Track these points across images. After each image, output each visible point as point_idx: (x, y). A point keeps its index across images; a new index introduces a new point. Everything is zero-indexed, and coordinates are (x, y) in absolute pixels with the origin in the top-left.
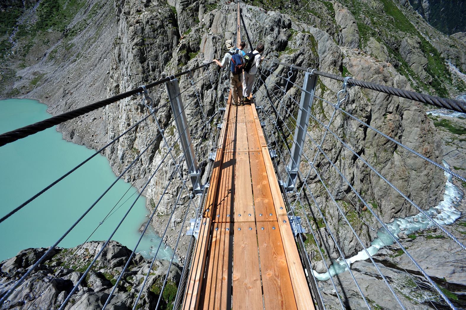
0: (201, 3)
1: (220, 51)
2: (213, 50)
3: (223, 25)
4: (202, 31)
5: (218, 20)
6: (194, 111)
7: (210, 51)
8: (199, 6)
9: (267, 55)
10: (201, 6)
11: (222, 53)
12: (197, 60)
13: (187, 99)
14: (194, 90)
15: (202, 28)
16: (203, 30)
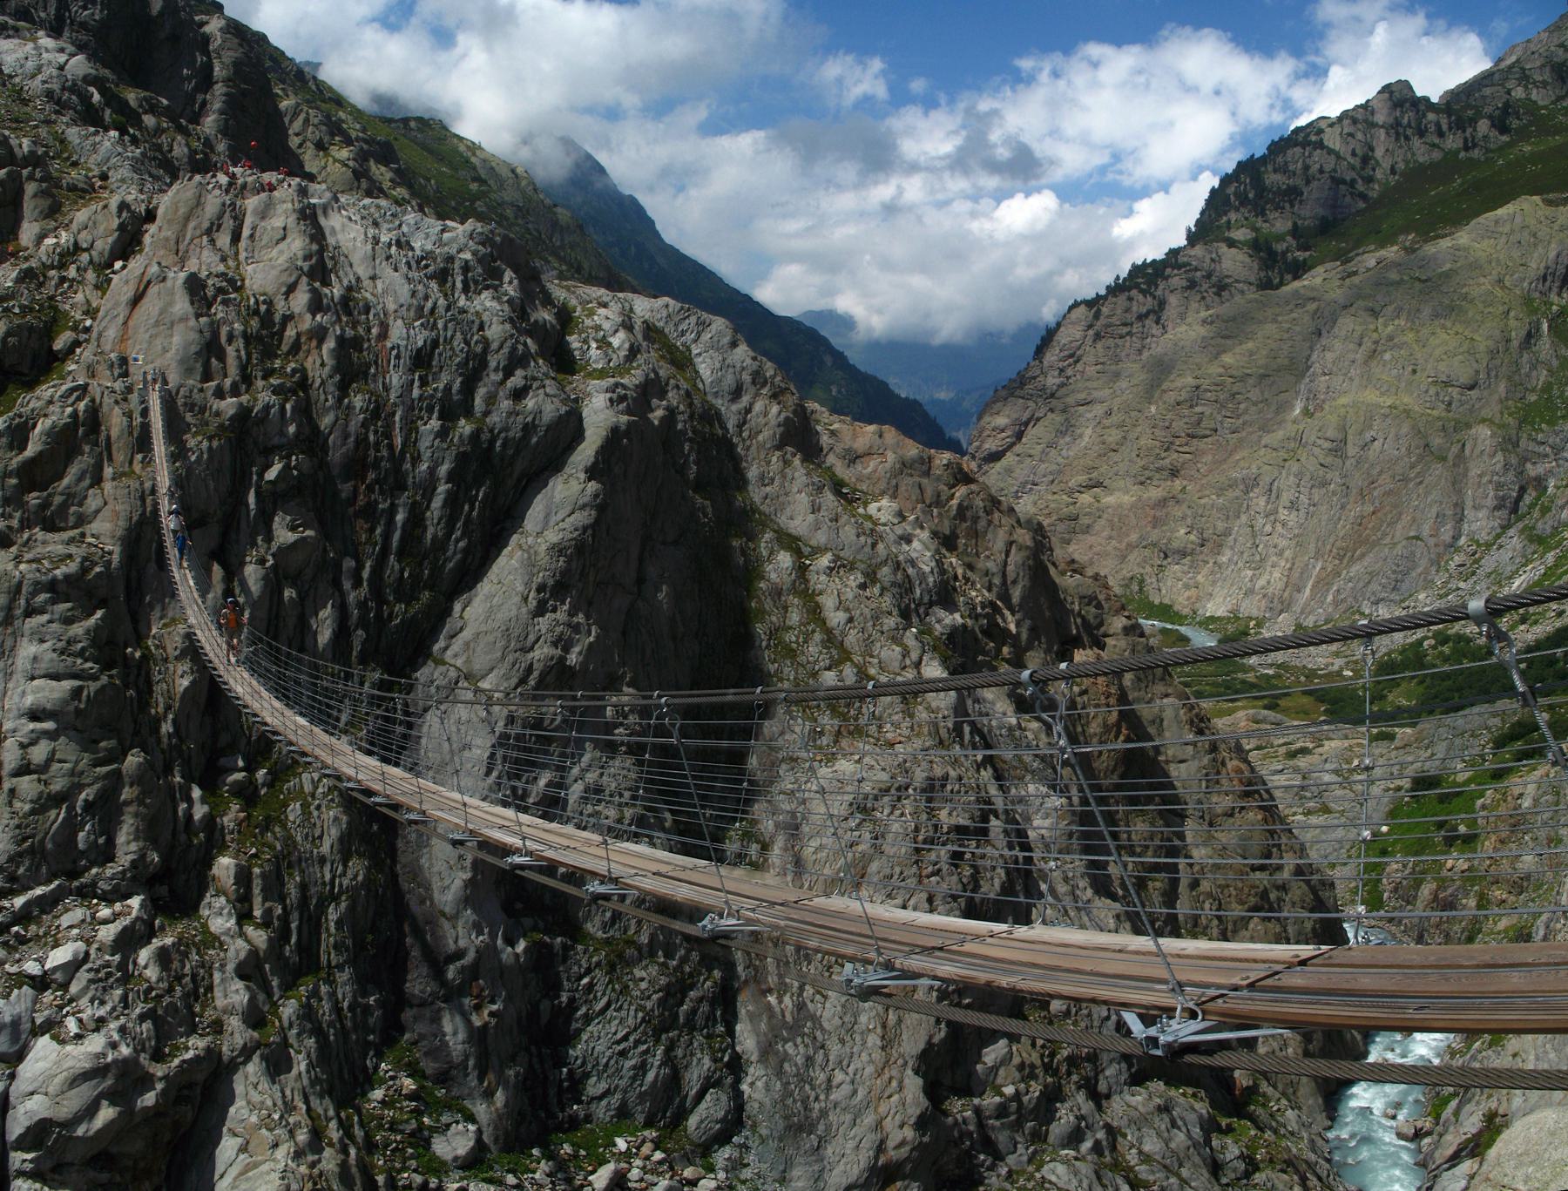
0: (31, 177)
1: (241, 343)
2: (194, 336)
3: (224, 240)
4: (63, 280)
5: (187, 219)
6: (93, 686)
7: (177, 340)
8: (20, 192)
9: (508, 373)
10: (30, 188)
11: (249, 355)
12: (84, 389)
13: (30, 612)
14: (78, 551)
15: (62, 266)
16: (72, 272)
